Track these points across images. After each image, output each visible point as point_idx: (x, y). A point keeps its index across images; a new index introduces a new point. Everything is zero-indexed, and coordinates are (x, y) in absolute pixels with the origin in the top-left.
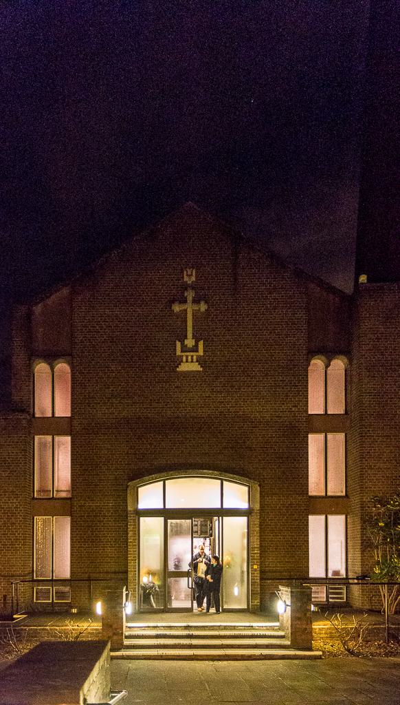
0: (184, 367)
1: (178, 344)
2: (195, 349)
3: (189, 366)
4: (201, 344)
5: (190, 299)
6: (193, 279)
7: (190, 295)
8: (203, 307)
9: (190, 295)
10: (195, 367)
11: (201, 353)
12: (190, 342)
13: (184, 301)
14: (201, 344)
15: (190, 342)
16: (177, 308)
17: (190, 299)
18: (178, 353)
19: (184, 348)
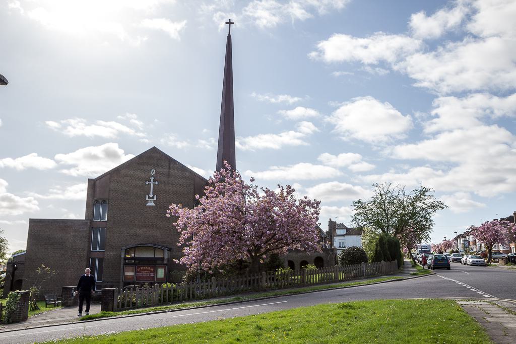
0: (149, 204)
1: (147, 196)
2: (153, 198)
3: (151, 204)
4: (155, 196)
5: (152, 180)
6: (154, 173)
7: (152, 179)
8: (157, 183)
9: (152, 179)
10: (153, 204)
11: (155, 199)
12: (151, 196)
13: (150, 181)
14: (155, 196)
15: (151, 196)
16: (147, 183)
17: (152, 180)
18: (147, 199)
19: (149, 198)
